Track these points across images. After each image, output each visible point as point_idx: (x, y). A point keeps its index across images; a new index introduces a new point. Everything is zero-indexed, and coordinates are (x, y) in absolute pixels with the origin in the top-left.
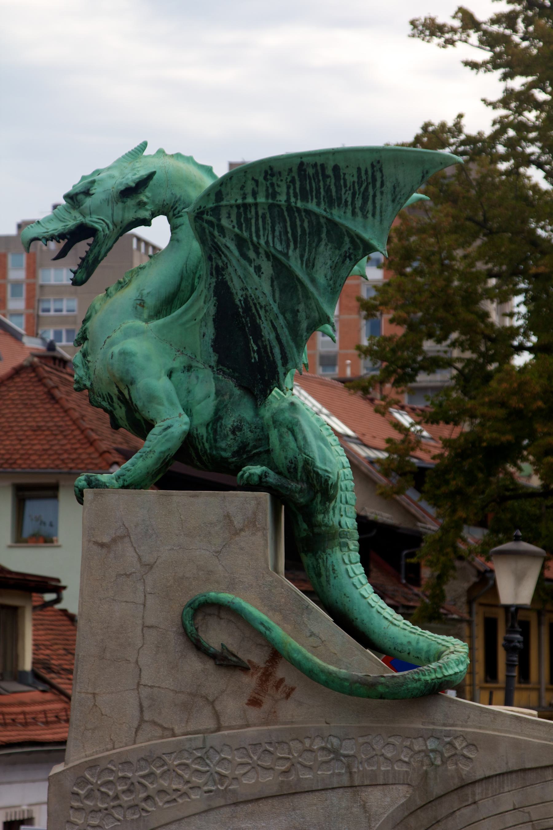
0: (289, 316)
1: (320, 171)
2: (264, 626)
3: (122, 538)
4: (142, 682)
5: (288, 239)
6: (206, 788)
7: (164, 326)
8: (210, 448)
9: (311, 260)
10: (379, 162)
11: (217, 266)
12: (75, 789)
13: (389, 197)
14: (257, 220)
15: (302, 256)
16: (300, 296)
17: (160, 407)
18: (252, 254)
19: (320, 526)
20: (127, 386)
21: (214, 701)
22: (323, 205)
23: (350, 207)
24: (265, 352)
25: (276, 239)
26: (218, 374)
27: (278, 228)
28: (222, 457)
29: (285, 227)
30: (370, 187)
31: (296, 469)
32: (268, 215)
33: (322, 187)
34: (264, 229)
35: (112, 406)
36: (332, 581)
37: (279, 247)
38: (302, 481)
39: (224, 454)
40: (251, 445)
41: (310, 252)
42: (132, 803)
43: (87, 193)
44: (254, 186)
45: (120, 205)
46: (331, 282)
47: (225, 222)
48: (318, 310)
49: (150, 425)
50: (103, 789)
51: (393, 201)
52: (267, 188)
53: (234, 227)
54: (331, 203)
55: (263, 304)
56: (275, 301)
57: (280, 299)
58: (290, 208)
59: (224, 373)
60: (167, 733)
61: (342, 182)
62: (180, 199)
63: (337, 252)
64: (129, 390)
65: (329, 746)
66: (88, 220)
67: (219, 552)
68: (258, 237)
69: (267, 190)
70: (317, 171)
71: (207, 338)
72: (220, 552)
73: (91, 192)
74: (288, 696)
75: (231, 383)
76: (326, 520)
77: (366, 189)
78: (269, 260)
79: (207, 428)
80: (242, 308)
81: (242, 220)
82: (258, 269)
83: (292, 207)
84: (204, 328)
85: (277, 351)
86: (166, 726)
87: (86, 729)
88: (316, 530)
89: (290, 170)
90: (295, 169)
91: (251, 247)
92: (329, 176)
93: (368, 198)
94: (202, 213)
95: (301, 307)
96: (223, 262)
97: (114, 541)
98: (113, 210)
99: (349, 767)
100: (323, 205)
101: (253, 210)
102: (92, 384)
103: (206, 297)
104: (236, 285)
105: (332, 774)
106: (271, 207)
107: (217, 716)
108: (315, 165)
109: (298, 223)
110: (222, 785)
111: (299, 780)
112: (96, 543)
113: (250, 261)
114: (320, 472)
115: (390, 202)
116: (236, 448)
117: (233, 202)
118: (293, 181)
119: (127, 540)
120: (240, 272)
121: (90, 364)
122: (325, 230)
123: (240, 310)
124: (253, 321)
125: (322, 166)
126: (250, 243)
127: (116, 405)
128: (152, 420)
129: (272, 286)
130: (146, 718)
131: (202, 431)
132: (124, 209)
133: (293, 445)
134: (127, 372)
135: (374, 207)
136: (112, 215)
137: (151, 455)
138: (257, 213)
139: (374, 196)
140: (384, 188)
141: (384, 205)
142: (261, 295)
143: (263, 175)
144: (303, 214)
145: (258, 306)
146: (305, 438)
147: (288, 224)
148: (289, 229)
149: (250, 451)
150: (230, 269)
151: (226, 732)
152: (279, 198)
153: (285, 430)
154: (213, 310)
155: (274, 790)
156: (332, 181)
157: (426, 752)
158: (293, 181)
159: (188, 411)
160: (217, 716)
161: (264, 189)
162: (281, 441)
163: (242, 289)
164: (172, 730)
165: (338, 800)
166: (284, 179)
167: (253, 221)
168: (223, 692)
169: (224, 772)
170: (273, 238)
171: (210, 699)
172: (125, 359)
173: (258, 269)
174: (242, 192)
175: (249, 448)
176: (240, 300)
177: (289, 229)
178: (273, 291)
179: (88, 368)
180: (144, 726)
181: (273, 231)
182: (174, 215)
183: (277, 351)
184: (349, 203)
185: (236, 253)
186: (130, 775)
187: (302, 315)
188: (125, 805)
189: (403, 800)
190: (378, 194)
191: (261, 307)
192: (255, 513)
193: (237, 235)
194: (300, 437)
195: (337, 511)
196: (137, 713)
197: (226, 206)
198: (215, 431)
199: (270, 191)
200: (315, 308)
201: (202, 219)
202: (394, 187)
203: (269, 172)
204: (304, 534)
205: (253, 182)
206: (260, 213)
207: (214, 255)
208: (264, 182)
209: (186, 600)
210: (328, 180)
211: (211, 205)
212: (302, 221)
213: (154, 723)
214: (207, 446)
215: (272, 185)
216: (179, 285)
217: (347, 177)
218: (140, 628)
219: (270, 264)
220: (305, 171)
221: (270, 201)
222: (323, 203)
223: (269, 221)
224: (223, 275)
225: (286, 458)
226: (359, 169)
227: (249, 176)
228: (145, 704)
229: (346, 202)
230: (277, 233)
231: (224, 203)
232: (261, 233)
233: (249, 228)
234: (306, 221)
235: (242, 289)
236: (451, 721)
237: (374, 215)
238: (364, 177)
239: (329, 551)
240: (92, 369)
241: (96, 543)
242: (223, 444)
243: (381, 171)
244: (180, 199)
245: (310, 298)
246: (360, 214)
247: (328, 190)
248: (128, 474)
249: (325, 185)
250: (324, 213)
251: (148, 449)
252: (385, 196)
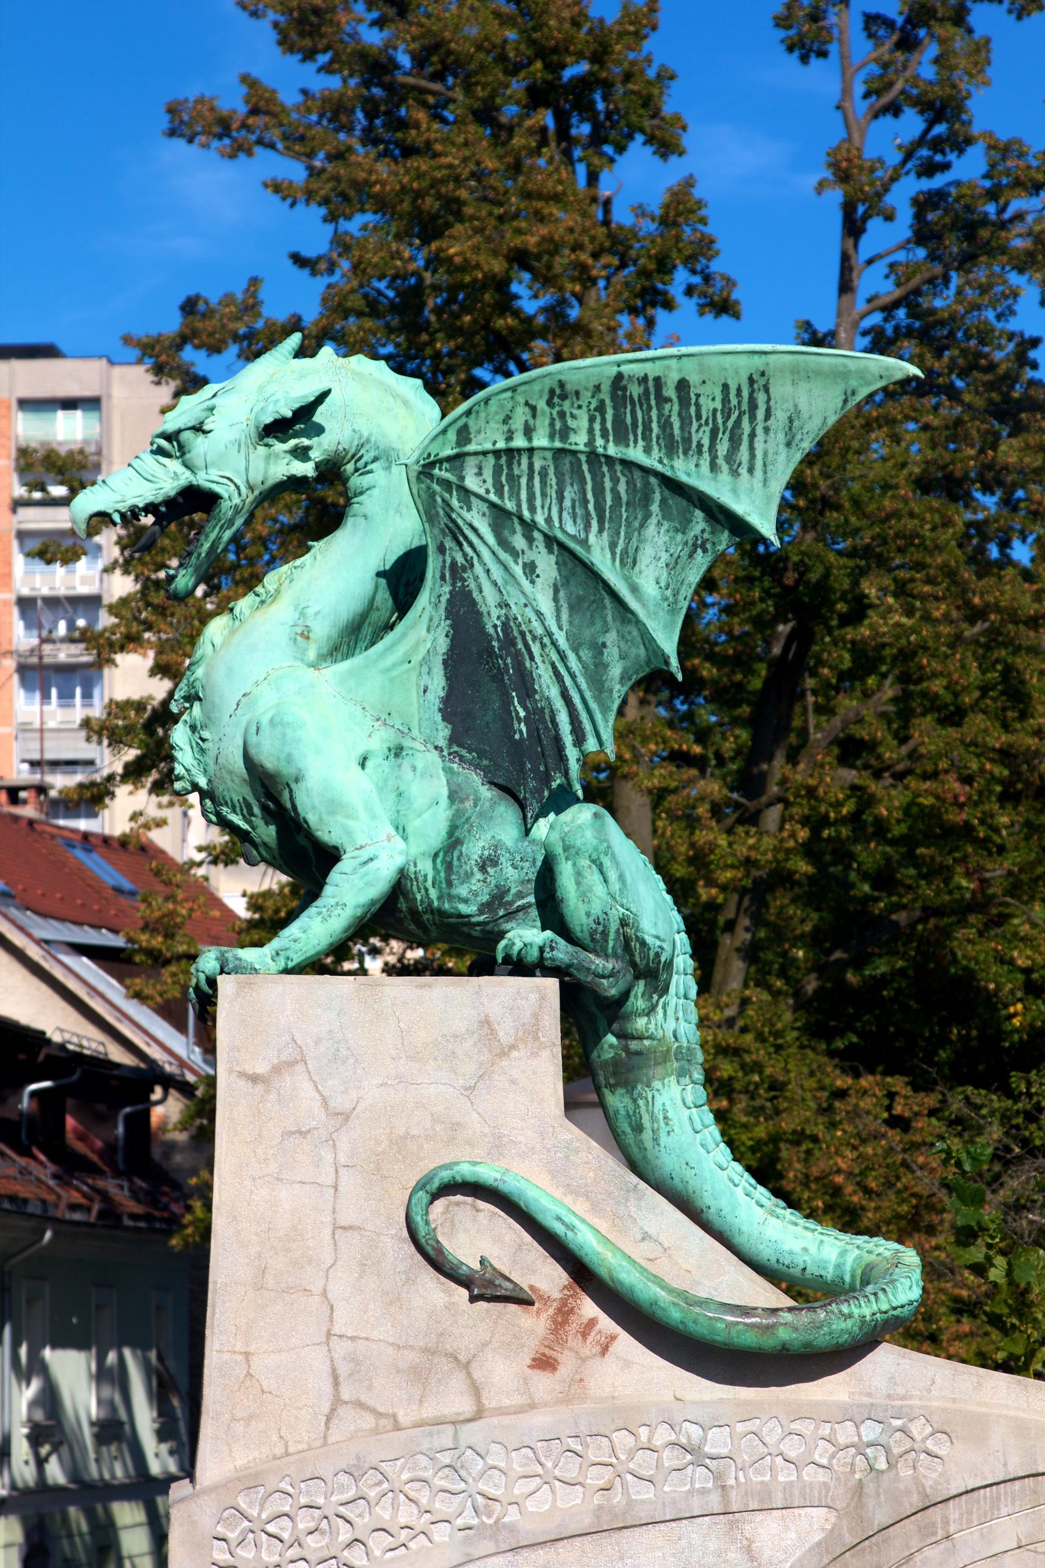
0: (586, 654)
1: (652, 390)
2: (563, 1223)
3: (291, 1064)
4: (336, 1330)
5: (588, 514)
6: (460, 1522)
7: (351, 672)
8: (439, 898)
9: (631, 552)
10: (763, 374)
11: (454, 563)
12: (219, 1528)
13: (781, 437)
14: (531, 478)
15: (613, 546)
16: (609, 618)
17: (350, 823)
18: (519, 541)
19: (641, 1038)
21: (469, 1362)
22: (656, 453)
23: (706, 456)
24: (541, 720)
25: (565, 514)
26: (451, 761)
27: (569, 494)
28: (460, 916)
29: (583, 492)
30: (746, 419)
31: (605, 934)
32: (551, 471)
33: (654, 418)
34: (544, 495)
36: (664, 1139)
37: (571, 529)
38: (615, 955)
39: (464, 909)
40: (513, 891)
41: (629, 538)
42: (326, 1554)
43: (198, 429)
44: (529, 417)
45: (262, 450)
46: (669, 593)
47: (471, 482)
49: (330, 856)
50: (271, 1528)
51: (788, 444)
52: (553, 419)
53: (488, 491)
54: (671, 448)
55: (539, 631)
56: (560, 628)
57: (571, 623)
58: (593, 456)
59: (462, 758)
60: (383, 1422)
61: (693, 410)
62: (368, 441)
63: (679, 537)
64: (291, 791)
65: (683, 1440)
66: (202, 480)
67: (472, 1089)
68: (532, 509)
69: (552, 424)
70: (647, 391)
71: (430, 695)
72: (472, 1089)
73: (206, 427)
74: (605, 1350)
75: (475, 779)
76: (652, 1027)
77: (738, 422)
78: (550, 551)
79: (434, 861)
80: (499, 640)
81: (503, 479)
82: (530, 569)
83: (598, 455)
84: (425, 677)
85: (563, 718)
86: (382, 1410)
87: (234, 1419)
88: (634, 1045)
89: (598, 388)
90: (606, 387)
91: (518, 527)
92: (669, 400)
93: (740, 440)
94: (432, 464)
96: (465, 555)
97: (277, 1070)
98: (248, 461)
99: (718, 1476)
100: (656, 453)
101: (525, 461)
102: (210, 781)
103: (431, 619)
104: (488, 599)
105: (691, 1492)
106: (559, 454)
107: (476, 1390)
108: (645, 379)
109: (608, 484)
110: (489, 1516)
111: (631, 1503)
112: (242, 1074)
113: (515, 554)
114: (649, 940)
115: (782, 447)
116: (485, 898)
117: (488, 446)
118: (601, 408)
119: (300, 1068)
120: (497, 573)
122: (657, 497)
123: (495, 644)
124: (519, 665)
125: (657, 380)
126: (516, 520)
128: (336, 848)
129: (556, 599)
130: (345, 1396)
131: (426, 867)
132: (268, 458)
133: (600, 890)
134: (289, 759)
135: (752, 456)
136: (247, 469)
137: (339, 911)
138: (531, 466)
139: (753, 435)
140: (771, 422)
141: (771, 451)
142: (533, 617)
143: (546, 397)
144: (618, 468)
145: (529, 637)
146: (621, 878)
147: (589, 487)
148: (590, 496)
149: (511, 903)
150: (478, 569)
151: (495, 1420)
152: (573, 438)
153: (584, 862)
154: (443, 644)
155: (586, 1523)
156: (673, 409)
157: (860, 1448)
158: (601, 408)
159: (401, 830)
160: (476, 1390)
161: (547, 422)
162: (578, 884)
163: (500, 606)
164: (394, 1416)
165: (702, 1538)
166: (585, 404)
167: (524, 481)
168: (485, 1344)
169: (492, 1492)
170: (561, 511)
171: (462, 1358)
172: (284, 735)
173: (530, 569)
174: (506, 428)
175: (509, 898)
176: (495, 626)
177: (590, 496)
178: (558, 610)
180: (341, 1411)
181: (561, 499)
182: (356, 470)
183: (563, 718)
184: (705, 448)
185: (491, 539)
186: (320, 1501)
187: (612, 653)
188: (313, 1558)
189: (818, 1537)
190: (759, 431)
191: (534, 638)
192: (536, 1016)
193: (493, 505)
194: (612, 875)
195: (670, 1011)
196: (328, 1388)
197: (476, 453)
198: (449, 867)
199: (558, 425)
201: (431, 476)
202: (791, 420)
203: (558, 392)
204: (608, 1055)
205: (527, 410)
206: (537, 465)
207: (449, 543)
208: (547, 409)
209: (412, 1179)
210: (667, 406)
211: (448, 452)
212: (615, 481)
213: (360, 1405)
214: (433, 894)
215: (562, 415)
216: (373, 599)
217: (702, 400)
218: (328, 1231)
219: (553, 559)
220: (624, 389)
221: (558, 444)
222: (655, 448)
223: (554, 482)
224: (464, 580)
225: (588, 914)
226: (725, 387)
227: (521, 400)
228: (343, 1370)
229: (700, 446)
230: (567, 503)
231: (471, 448)
232: (538, 502)
233: (515, 494)
234: (623, 480)
235: (500, 606)
236: (901, 1391)
237: (751, 470)
238: (734, 401)
239: (657, 1084)
240: (212, 754)
241: (242, 1074)
242: (463, 891)
243: (767, 390)
244: (368, 441)
246: (725, 468)
247: (666, 425)
248: (297, 946)
249: (660, 416)
250: (659, 468)
251: (332, 901)
252: (772, 434)
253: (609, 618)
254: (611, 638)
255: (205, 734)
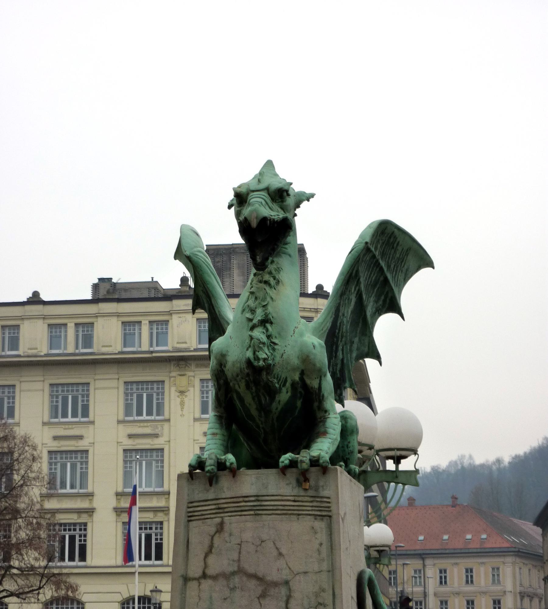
16: (358, 332)
20: (321, 377)
35: (280, 389)
48: (369, 347)
55: (344, 330)
78: (356, 297)
95: (356, 340)
102: (274, 365)
121: (276, 347)
127: (284, 390)
144: (378, 269)
179: (274, 349)
187: (355, 346)
200: (367, 344)
212: (374, 274)
245: (366, 335)
253: (358, 332)
254: (356, 340)
255: (274, 340)
